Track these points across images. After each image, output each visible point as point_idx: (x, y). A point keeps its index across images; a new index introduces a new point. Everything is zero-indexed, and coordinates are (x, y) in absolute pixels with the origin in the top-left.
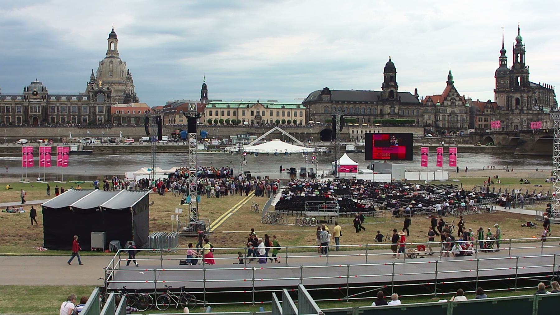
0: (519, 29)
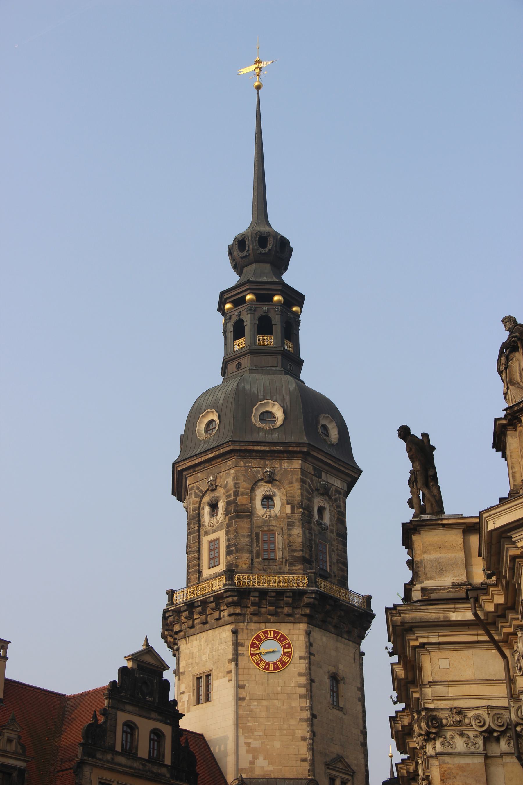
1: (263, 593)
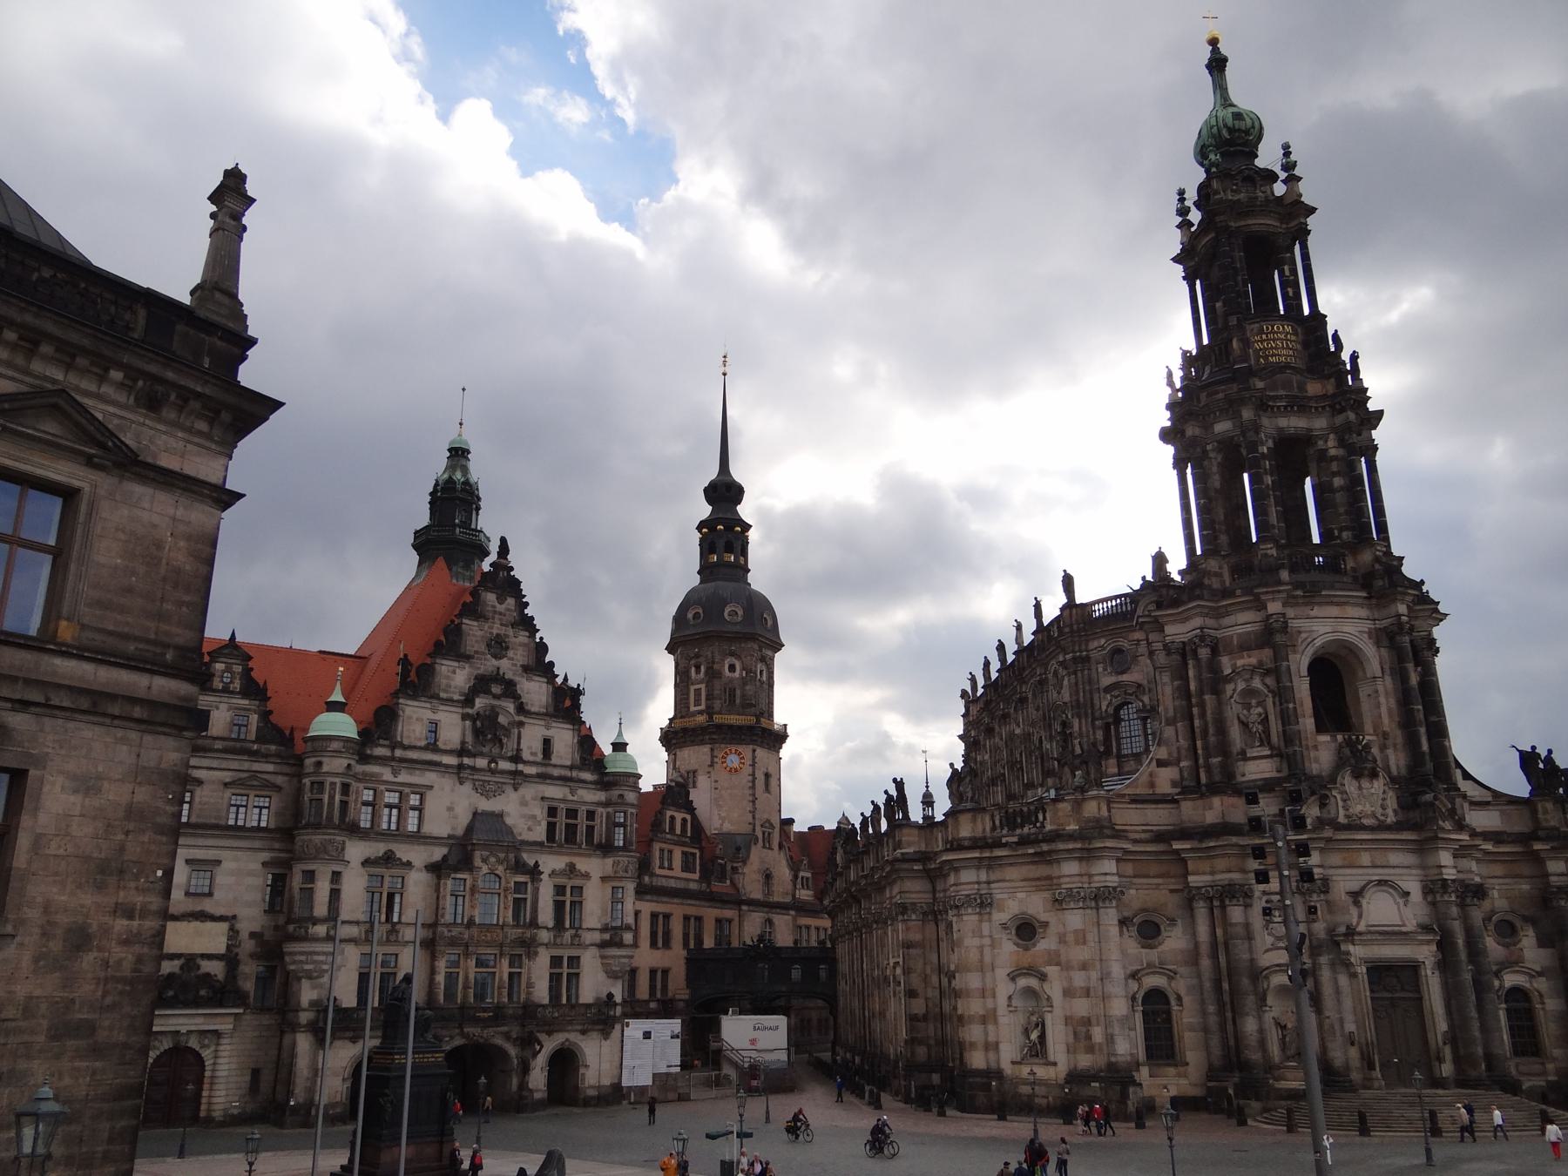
0: (1217, 64)
1: (730, 727)
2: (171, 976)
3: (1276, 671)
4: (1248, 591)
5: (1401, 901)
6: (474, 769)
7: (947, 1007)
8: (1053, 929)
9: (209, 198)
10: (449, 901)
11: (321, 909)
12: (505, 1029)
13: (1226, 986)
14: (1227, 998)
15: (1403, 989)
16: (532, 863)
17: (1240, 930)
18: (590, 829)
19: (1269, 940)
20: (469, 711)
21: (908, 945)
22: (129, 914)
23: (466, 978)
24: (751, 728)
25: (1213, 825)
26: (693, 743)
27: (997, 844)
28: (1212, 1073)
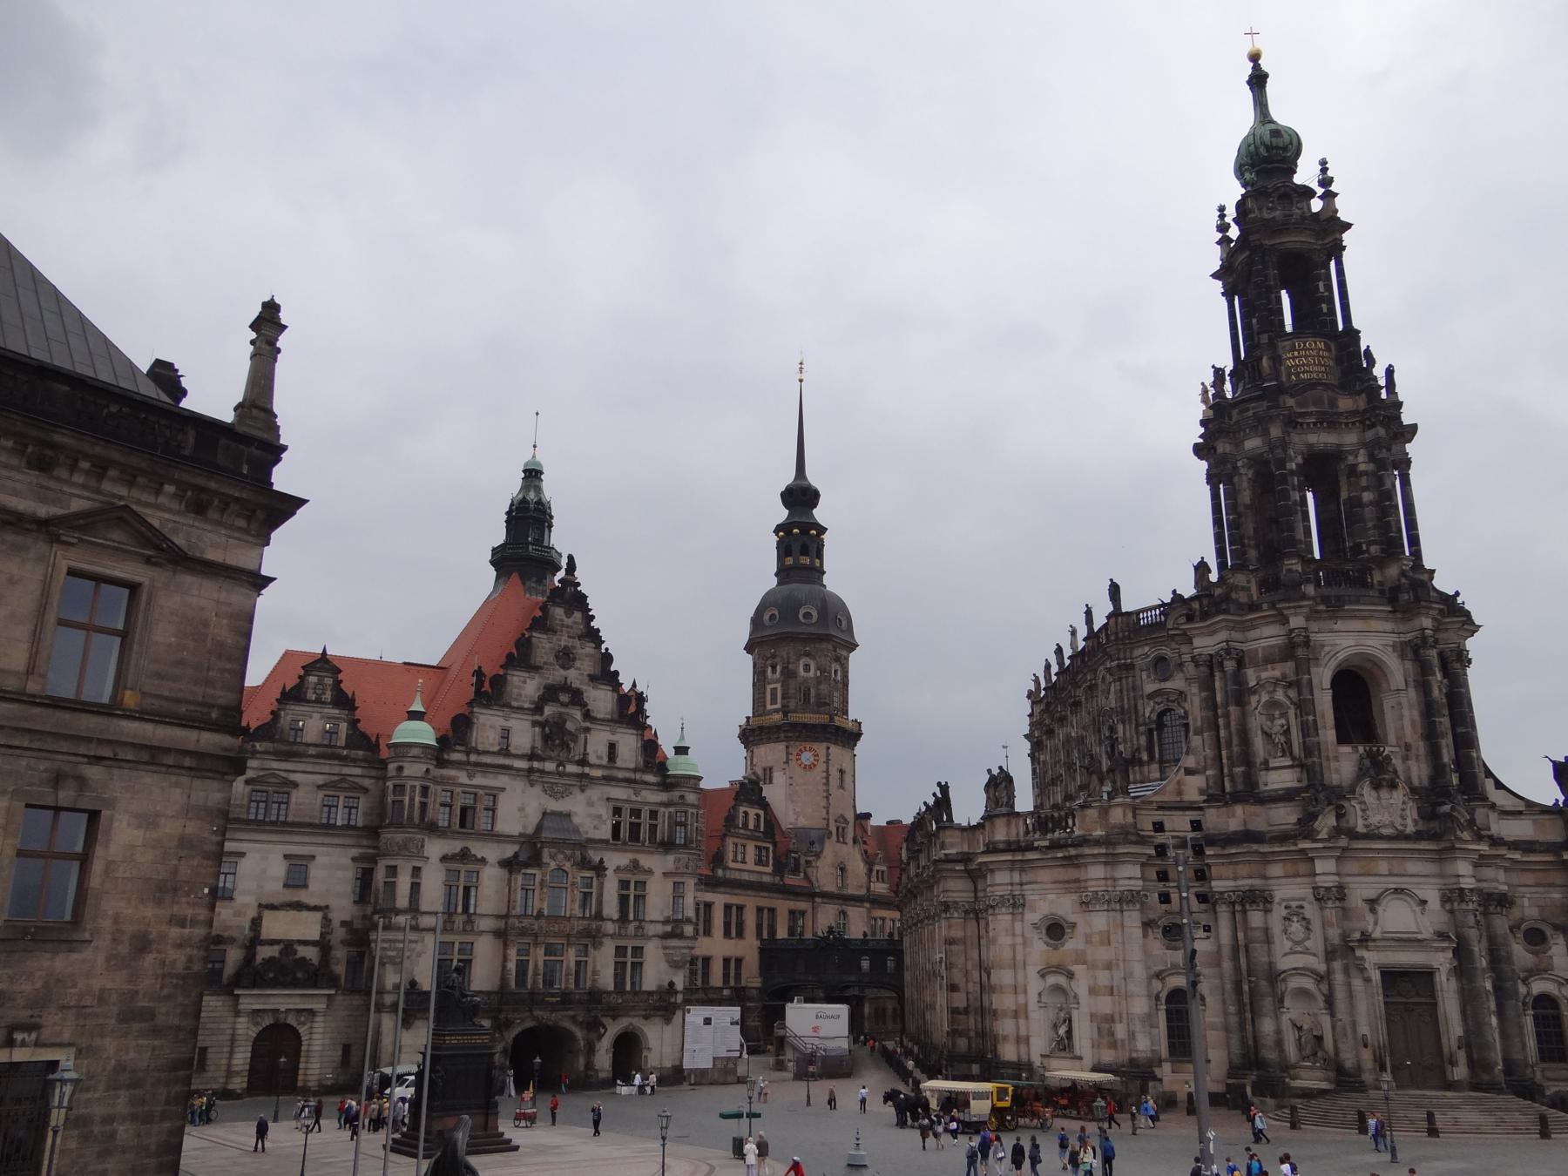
0: (1258, 81)
1: (805, 725)
2: (272, 959)
3: (1299, 685)
4: (1273, 606)
5: (1418, 909)
6: (542, 772)
7: (986, 1004)
8: (1080, 930)
9: (251, 326)
10: (519, 895)
11: (402, 901)
12: (571, 1013)
13: (1246, 987)
14: (1246, 1000)
15: (1418, 994)
16: (597, 859)
17: (1258, 934)
18: (653, 828)
19: (1288, 944)
20: (537, 718)
21: (950, 942)
22: (182, 923)
23: (536, 966)
24: (824, 727)
25: (1235, 833)
26: (769, 740)
27: (1030, 848)
28: (1234, 1070)
